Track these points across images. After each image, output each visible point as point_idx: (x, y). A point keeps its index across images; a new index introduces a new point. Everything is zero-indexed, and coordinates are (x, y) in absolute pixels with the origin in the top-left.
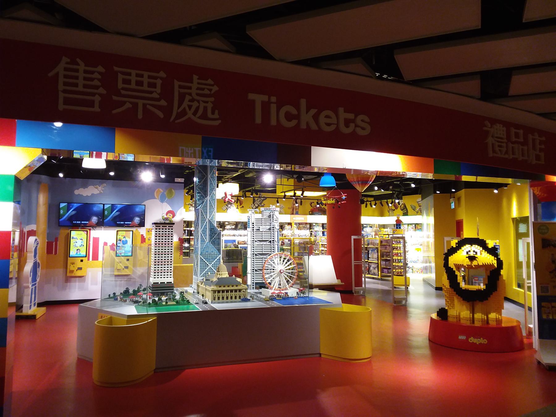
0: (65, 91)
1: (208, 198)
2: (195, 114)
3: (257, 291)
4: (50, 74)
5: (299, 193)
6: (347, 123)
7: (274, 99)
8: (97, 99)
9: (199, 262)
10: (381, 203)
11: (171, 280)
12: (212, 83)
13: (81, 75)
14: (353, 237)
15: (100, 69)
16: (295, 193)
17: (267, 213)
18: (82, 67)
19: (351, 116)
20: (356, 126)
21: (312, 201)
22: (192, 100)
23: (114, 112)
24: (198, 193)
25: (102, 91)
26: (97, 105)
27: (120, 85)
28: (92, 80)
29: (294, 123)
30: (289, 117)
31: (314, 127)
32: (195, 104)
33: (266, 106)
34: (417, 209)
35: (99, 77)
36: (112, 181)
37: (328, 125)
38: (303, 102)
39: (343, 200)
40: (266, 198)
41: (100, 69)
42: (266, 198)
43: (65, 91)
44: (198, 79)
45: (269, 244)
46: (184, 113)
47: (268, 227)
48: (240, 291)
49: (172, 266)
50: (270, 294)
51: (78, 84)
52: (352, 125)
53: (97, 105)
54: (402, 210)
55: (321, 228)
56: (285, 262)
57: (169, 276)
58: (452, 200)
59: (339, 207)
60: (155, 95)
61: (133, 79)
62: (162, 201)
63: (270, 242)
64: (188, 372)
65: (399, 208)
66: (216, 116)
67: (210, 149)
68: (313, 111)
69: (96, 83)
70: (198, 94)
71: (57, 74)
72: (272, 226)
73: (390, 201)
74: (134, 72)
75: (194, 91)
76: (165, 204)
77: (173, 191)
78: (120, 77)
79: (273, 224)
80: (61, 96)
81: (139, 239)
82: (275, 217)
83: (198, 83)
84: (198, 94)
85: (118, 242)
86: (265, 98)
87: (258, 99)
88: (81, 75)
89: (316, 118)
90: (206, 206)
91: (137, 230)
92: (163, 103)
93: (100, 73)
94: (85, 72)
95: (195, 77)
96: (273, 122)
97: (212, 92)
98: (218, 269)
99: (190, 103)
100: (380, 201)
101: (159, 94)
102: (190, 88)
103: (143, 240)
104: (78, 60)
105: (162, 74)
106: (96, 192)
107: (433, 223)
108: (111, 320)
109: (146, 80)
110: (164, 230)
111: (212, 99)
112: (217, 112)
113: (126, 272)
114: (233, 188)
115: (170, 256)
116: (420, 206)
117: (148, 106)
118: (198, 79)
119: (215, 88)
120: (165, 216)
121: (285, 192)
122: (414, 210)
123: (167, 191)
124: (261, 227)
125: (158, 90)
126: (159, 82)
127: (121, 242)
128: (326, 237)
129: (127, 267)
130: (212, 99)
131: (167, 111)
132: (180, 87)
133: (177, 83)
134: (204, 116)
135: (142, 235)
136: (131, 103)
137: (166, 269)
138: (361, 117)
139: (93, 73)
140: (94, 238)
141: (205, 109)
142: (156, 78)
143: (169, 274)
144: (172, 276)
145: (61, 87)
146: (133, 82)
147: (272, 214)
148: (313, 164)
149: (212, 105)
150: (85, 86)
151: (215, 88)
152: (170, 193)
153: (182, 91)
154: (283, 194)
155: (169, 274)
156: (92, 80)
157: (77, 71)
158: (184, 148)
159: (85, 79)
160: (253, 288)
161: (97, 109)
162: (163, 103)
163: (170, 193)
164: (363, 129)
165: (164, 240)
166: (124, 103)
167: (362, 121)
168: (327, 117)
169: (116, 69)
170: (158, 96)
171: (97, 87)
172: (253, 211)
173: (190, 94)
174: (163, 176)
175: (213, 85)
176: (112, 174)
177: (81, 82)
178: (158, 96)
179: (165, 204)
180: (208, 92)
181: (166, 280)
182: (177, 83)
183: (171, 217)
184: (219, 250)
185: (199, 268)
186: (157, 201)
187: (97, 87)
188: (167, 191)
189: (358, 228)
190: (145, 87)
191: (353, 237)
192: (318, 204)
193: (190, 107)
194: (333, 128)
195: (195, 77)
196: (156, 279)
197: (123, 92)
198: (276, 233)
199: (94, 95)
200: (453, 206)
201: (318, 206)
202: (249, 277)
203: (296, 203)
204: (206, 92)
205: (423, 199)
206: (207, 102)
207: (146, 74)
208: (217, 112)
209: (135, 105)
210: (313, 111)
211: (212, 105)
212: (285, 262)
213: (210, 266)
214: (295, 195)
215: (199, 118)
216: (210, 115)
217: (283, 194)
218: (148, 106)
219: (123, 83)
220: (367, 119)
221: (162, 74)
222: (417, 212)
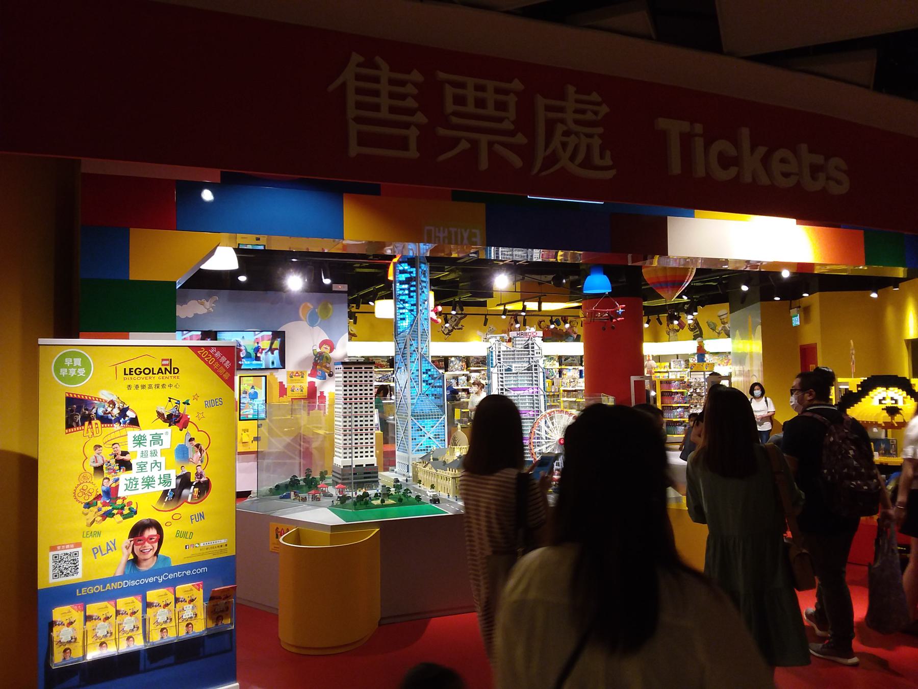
0: (358, 120)
2: (572, 158)
4: (331, 88)
5: (532, 306)
6: (815, 170)
7: (699, 128)
8: (413, 134)
10: (658, 319)
11: (373, 461)
12: (599, 99)
13: (384, 87)
14: (633, 378)
15: (416, 76)
16: (524, 307)
17: (520, 342)
18: (385, 72)
19: (819, 159)
20: (828, 178)
22: (567, 134)
23: (442, 158)
25: (420, 118)
26: (413, 144)
27: (450, 107)
28: (403, 97)
29: (733, 172)
30: (725, 162)
31: (764, 180)
32: (572, 140)
33: (686, 140)
35: (415, 91)
37: (786, 175)
38: (745, 132)
39: (618, 316)
40: (466, 315)
41: (416, 76)
42: (466, 315)
43: (358, 120)
44: (576, 92)
46: (552, 159)
47: (526, 365)
49: (373, 436)
51: (357, 108)
52: (822, 176)
53: (413, 144)
54: (692, 330)
56: (551, 425)
58: (793, 311)
59: (613, 328)
60: (507, 125)
61: (470, 94)
62: (312, 323)
64: (436, 623)
65: (686, 328)
66: (608, 161)
67: (473, 231)
68: (762, 150)
69: (411, 103)
70: (577, 122)
71: (344, 85)
74: (471, 82)
75: (569, 116)
76: (317, 329)
77: (330, 306)
78: (449, 91)
79: (535, 359)
80: (354, 129)
81: (276, 391)
82: (536, 347)
83: (577, 101)
84: (577, 122)
85: (243, 395)
86: (685, 126)
87: (673, 127)
88: (384, 87)
89: (765, 161)
91: (271, 374)
92: (520, 139)
93: (415, 84)
94: (392, 82)
95: (571, 89)
96: (700, 172)
97: (600, 117)
99: (565, 139)
100: (656, 316)
101: (513, 122)
102: (561, 110)
103: (283, 390)
104: (378, 60)
105: (517, 85)
107: (760, 351)
108: (298, 538)
109: (490, 97)
111: (600, 130)
112: (608, 153)
116: (723, 323)
117: (497, 147)
118: (576, 92)
119: (604, 109)
120: (318, 350)
121: (505, 305)
124: (514, 365)
125: (512, 113)
126: (512, 100)
127: (247, 396)
128: (583, 379)
130: (600, 130)
131: (527, 153)
132: (548, 108)
133: (541, 102)
134: (587, 163)
135: (281, 383)
136: (469, 140)
137: (364, 441)
138: (835, 161)
139: (402, 83)
141: (589, 147)
142: (506, 92)
143: (369, 450)
145: (352, 112)
146: (471, 101)
147: (530, 342)
148: (671, 252)
149: (600, 142)
150: (393, 110)
151: (604, 109)
152: (326, 309)
153: (552, 115)
154: (502, 308)
155: (369, 450)
156: (403, 97)
157: (376, 80)
158: (433, 228)
159: (392, 96)
161: (413, 153)
162: (520, 139)
163: (326, 309)
164: (839, 182)
165: (358, 392)
166: (456, 141)
167: (836, 168)
168: (783, 161)
169: (442, 75)
170: (512, 127)
171: (410, 112)
172: (498, 338)
173: (562, 121)
175: (599, 104)
176: (242, 279)
177: (384, 101)
178: (512, 127)
179: (317, 328)
180: (593, 117)
181: (364, 461)
182: (541, 102)
183: (327, 351)
186: (304, 325)
187: (410, 112)
189: (637, 362)
190: (491, 111)
191: (633, 378)
192: (552, 323)
193: (564, 145)
194: (791, 182)
195: (571, 89)
196: (348, 459)
197: (455, 120)
198: (541, 375)
199: (407, 126)
200: (796, 321)
201: (552, 327)
203: (517, 322)
204: (589, 116)
206: (589, 136)
207: (491, 85)
208: (608, 153)
209: (475, 144)
210: (762, 150)
211: (600, 142)
212: (551, 425)
214: (524, 309)
215: (580, 165)
216: (597, 161)
217: (502, 308)
218: (497, 147)
219: (454, 104)
220: (843, 165)
221: (517, 85)
222: (719, 333)
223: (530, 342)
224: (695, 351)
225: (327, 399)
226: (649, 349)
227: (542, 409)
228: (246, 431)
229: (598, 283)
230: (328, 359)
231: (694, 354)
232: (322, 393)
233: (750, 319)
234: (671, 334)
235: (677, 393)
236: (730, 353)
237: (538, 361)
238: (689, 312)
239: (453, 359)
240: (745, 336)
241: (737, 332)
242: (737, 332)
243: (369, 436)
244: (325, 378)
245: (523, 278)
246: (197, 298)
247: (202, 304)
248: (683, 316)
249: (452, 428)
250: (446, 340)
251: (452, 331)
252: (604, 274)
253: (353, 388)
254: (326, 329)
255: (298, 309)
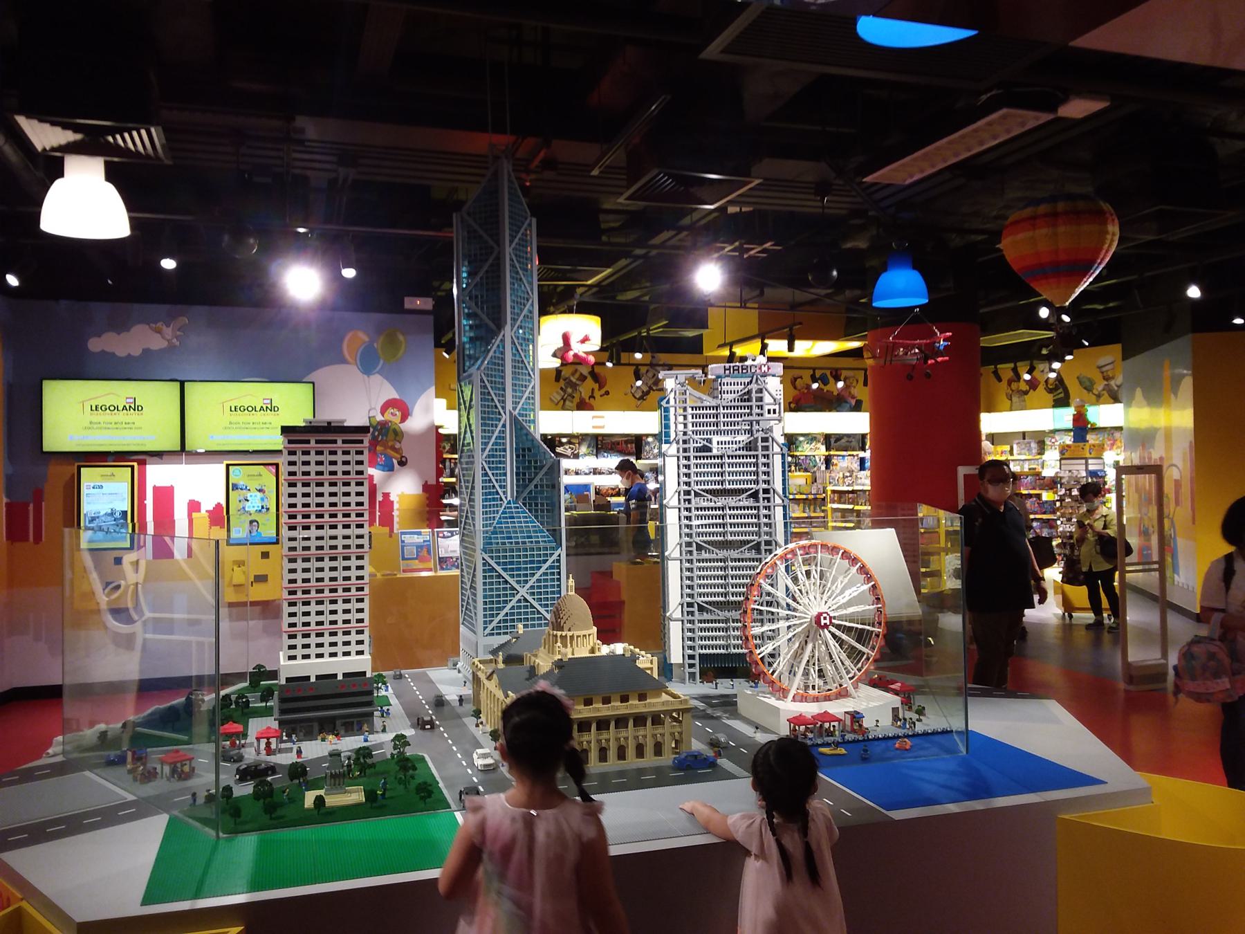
1: (508, 331)
3: (707, 689)
9: (479, 574)
10: (996, 373)
11: (362, 663)
21: (797, 373)
24: (469, 316)
34: (1100, 386)
36: (206, 308)
39: (939, 353)
45: (751, 502)
47: (744, 438)
48: (657, 719)
50: (785, 731)
54: (1050, 391)
55: (823, 448)
57: (353, 648)
59: (928, 376)
62: (368, 365)
63: (755, 495)
65: (1041, 388)
72: (760, 435)
73: (1023, 367)
76: (377, 379)
77: (401, 338)
79: (763, 425)
90: (499, 363)
98: (557, 614)
106: (157, 343)
110: (326, 458)
113: (259, 593)
114: (585, 331)
115: (353, 563)
116: (1107, 379)
120: (379, 418)
121: (731, 345)
122: (1089, 389)
123: (381, 339)
124: (715, 439)
128: (867, 473)
129: (261, 579)
140: (156, 489)
143: (353, 638)
144: (365, 647)
147: (754, 387)
152: (392, 341)
154: (726, 353)
155: (353, 638)
160: (692, 675)
163: (392, 341)
174: (349, 273)
181: (340, 665)
183: (397, 419)
184: (555, 533)
185: (480, 599)
186: (351, 372)
188: (381, 339)
191: (962, 471)
196: (299, 661)
201: (815, 386)
202: (675, 632)
205: (1125, 357)
213: (523, 592)
222: (1099, 396)
223: (754, 387)
224: (1070, 425)
225: (396, 506)
226: (989, 422)
227: (780, 538)
228: (240, 564)
229: (901, 288)
230: (398, 434)
231: (1069, 430)
232: (386, 495)
233: (1167, 373)
234: (1015, 399)
235: (1030, 496)
236: (1120, 429)
237: (771, 430)
238: (1051, 358)
239: (650, 439)
240: (1156, 395)
241: (1139, 392)
242: (1139, 392)
243: (354, 605)
244: (391, 469)
245: (762, 293)
246: (146, 321)
247: (159, 332)
248: (1041, 366)
249: (620, 568)
250: (638, 408)
251: (648, 393)
252: (914, 268)
253: (313, 490)
254: (393, 377)
255: (341, 340)
